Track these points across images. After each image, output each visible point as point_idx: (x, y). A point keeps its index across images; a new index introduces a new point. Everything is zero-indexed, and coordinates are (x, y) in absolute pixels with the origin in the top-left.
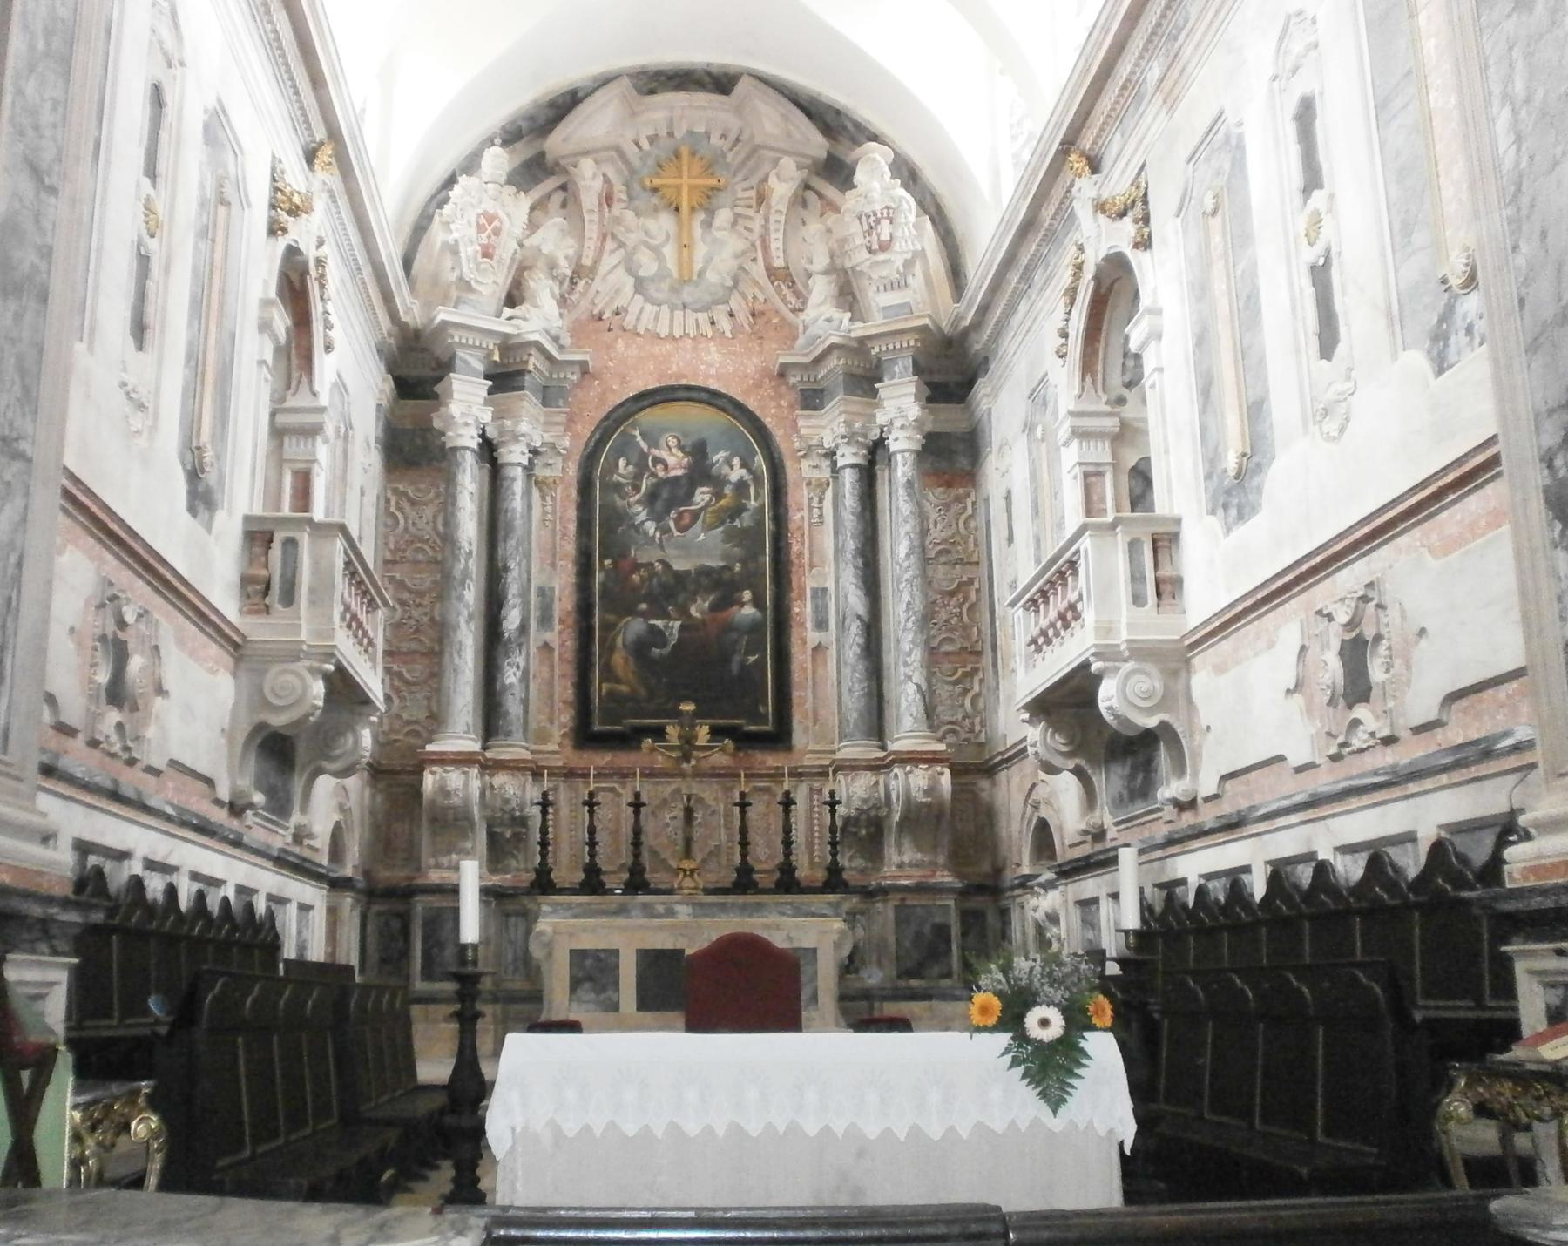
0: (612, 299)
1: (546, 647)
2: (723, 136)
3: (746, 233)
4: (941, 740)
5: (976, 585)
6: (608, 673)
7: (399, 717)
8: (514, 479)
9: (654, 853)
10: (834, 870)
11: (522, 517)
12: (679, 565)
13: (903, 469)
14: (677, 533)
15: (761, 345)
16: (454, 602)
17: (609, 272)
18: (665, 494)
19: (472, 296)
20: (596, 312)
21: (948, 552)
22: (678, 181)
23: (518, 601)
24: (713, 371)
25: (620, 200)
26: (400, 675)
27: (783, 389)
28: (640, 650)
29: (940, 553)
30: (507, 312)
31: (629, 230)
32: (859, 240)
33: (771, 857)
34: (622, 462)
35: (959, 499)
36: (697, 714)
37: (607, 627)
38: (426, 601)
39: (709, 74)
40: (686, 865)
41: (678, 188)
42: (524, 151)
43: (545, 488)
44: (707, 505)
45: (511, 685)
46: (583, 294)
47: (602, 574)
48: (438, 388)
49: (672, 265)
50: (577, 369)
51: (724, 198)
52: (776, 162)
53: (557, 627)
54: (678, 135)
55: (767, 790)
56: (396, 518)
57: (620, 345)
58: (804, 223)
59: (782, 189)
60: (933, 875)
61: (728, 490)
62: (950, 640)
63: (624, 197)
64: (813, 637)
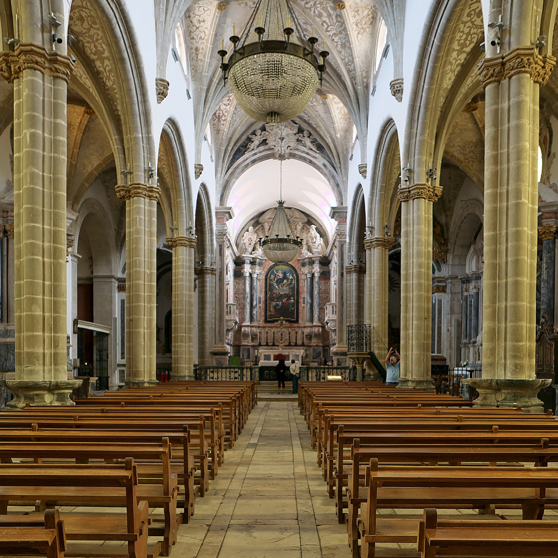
1: (260, 307)
6: (270, 311)
12: (281, 293)
13: (316, 279)
28: (275, 307)
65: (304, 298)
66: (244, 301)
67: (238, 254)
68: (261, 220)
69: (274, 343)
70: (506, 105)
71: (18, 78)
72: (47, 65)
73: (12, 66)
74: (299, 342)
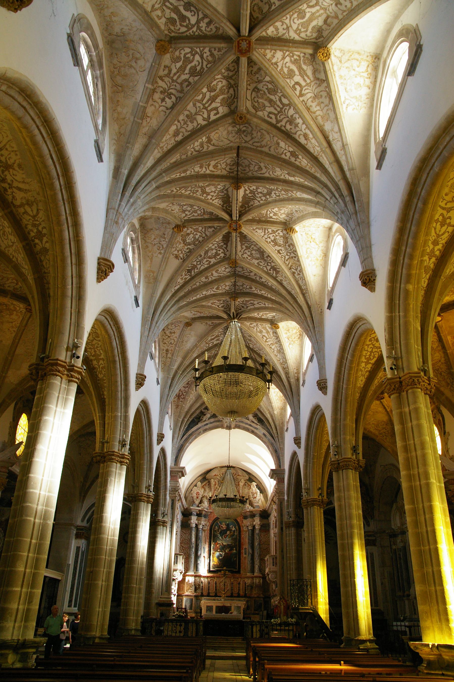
10: (246, 594)
37: (213, 553)
64: (244, 556)
65: (246, 549)
66: (190, 550)
67: (186, 506)
68: (208, 476)
69: (216, 593)
70: (407, 410)
71: (42, 380)
72: (66, 373)
73: (40, 372)
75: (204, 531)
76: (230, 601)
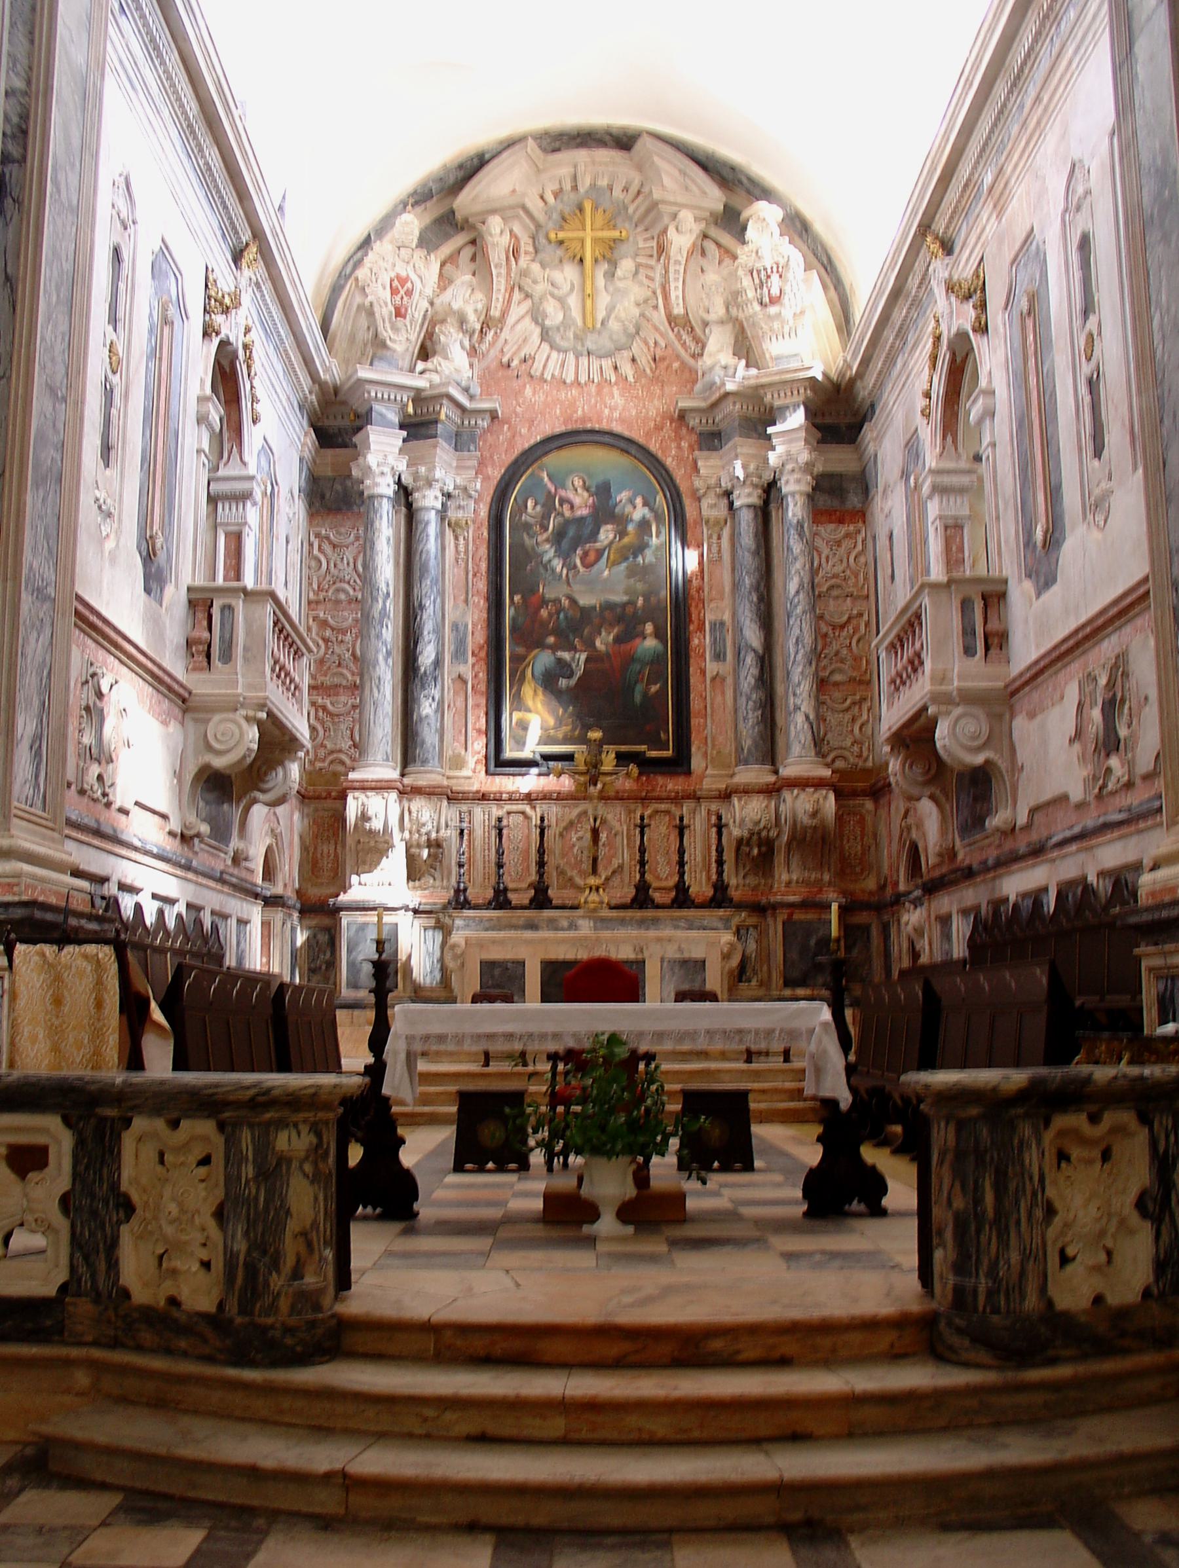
0: (519, 349)
2: (626, 189)
3: (646, 281)
4: (828, 765)
5: (866, 617)
7: (322, 745)
8: (427, 523)
9: (561, 873)
11: (436, 558)
12: (584, 601)
14: (581, 569)
15: (662, 389)
16: (373, 639)
17: (518, 321)
18: (571, 532)
19: (388, 353)
20: (505, 360)
21: (838, 586)
22: (580, 234)
23: (432, 637)
24: (616, 415)
25: (526, 253)
26: (324, 708)
27: (684, 431)
29: (832, 587)
30: (420, 366)
31: (535, 282)
32: (751, 294)
33: (670, 875)
34: (530, 503)
35: (847, 535)
36: (601, 743)
37: (517, 659)
38: (348, 638)
39: (611, 135)
40: (593, 881)
41: (582, 241)
42: (432, 211)
43: (459, 531)
44: (611, 543)
45: (427, 716)
46: (492, 344)
47: (513, 609)
48: (356, 439)
49: (576, 314)
50: (488, 416)
51: (624, 248)
52: (674, 216)
53: (471, 660)
54: (582, 190)
55: (668, 812)
56: (320, 562)
57: (528, 391)
58: (702, 271)
59: (681, 241)
60: (820, 891)
61: (631, 528)
62: (841, 671)
63: (531, 249)
64: (712, 667)
74: (700, 887)
75: (455, 526)
76: (633, 932)
